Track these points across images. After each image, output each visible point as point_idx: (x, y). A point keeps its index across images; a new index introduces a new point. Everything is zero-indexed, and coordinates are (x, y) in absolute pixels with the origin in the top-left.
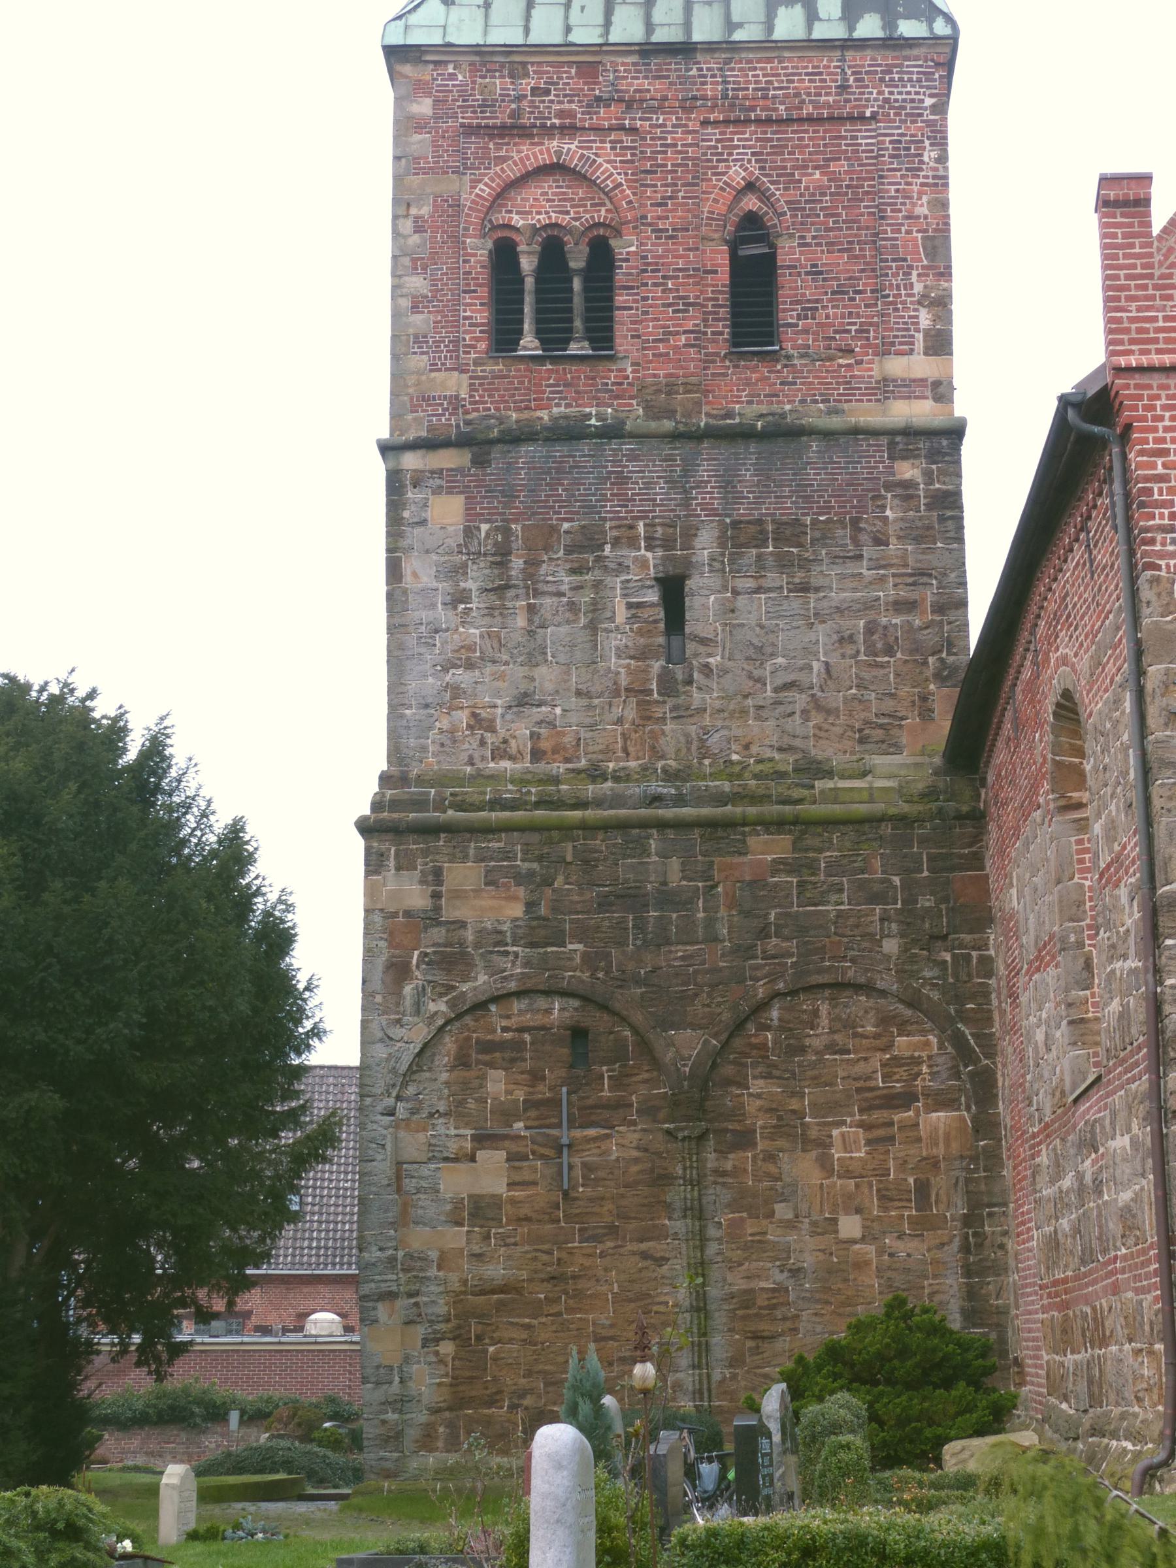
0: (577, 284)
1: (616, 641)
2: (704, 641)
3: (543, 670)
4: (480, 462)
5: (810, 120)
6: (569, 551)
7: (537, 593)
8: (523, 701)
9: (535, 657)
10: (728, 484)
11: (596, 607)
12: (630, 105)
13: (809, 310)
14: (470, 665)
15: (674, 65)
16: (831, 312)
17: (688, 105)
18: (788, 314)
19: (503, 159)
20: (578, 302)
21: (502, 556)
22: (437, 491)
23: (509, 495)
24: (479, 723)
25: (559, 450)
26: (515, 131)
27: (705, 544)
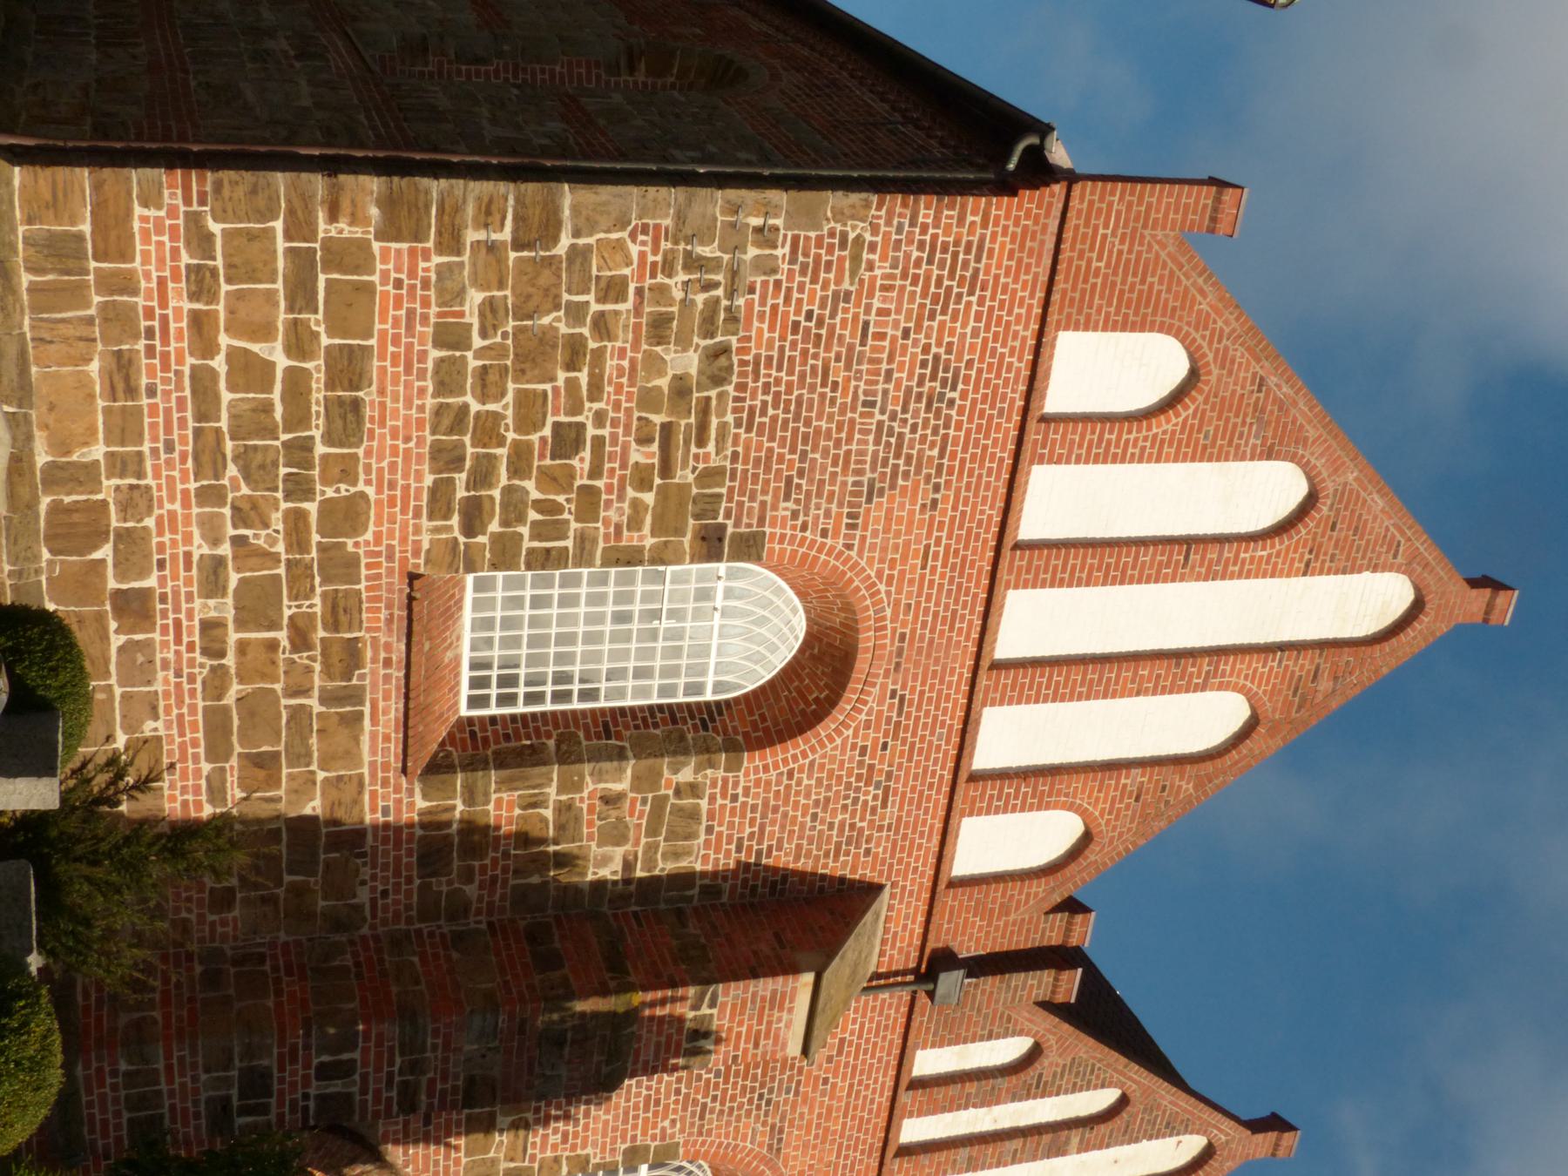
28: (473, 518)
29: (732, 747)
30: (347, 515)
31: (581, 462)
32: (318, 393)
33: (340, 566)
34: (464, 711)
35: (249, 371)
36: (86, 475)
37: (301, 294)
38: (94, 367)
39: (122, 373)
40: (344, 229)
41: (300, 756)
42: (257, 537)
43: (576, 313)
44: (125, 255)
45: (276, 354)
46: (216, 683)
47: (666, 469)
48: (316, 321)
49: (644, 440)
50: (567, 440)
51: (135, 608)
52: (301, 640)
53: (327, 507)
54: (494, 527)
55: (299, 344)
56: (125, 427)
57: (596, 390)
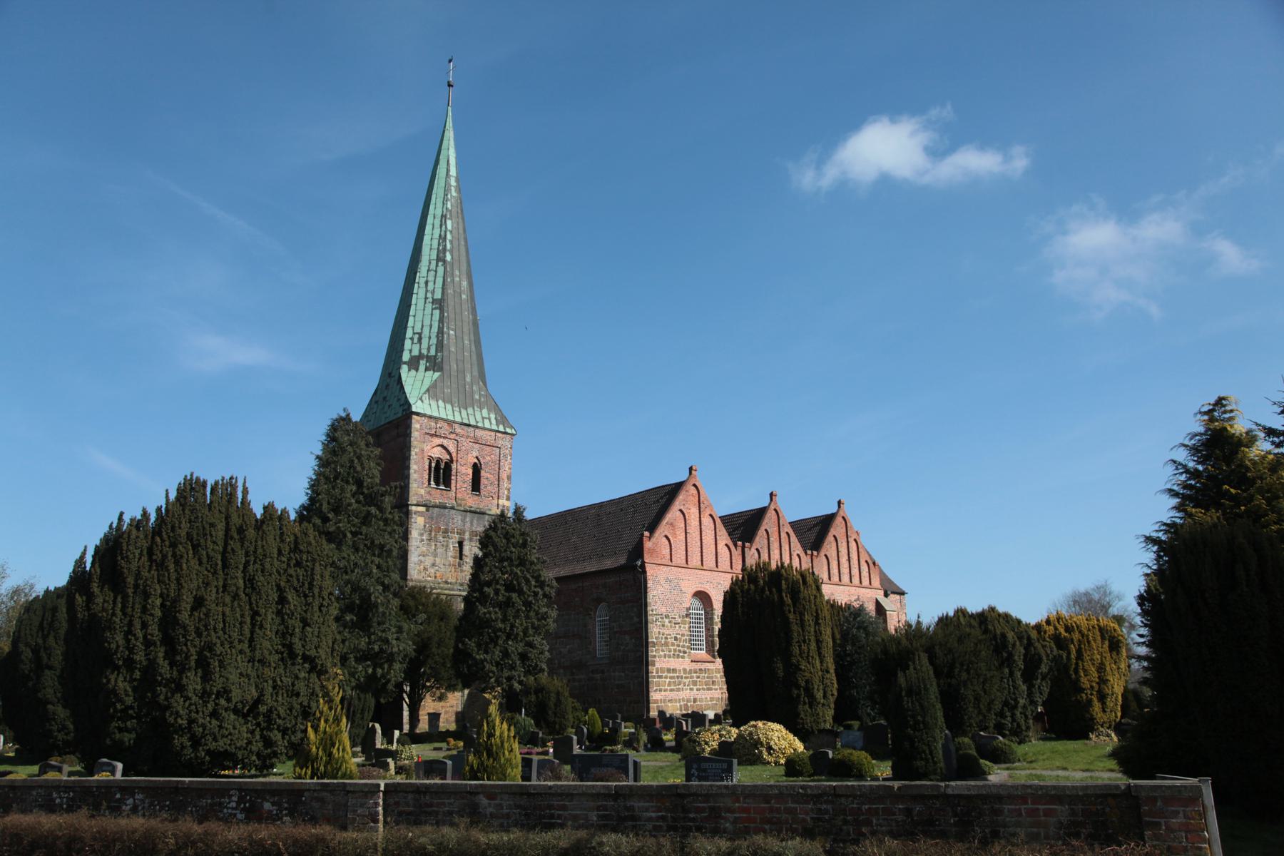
1: (450, 554)
4: (427, 510)
8: (434, 565)
9: (435, 555)
10: (472, 523)
11: (447, 546)
12: (457, 435)
13: (486, 487)
14: (424, 556)
15: (466, 428)
16: (490, 488)
17: (468, 437)
18: (482, 487)
21: (431, 531)
24: (425, 569)
25: (442, 510)
27: (467, 536)
28: (685, 652)
29: (712, 610)
30: (685, 670)
31: (678, 636)
32: (671, 675)
33: (690, 672)
35: (669, 684)
36: (681, 706)
37: (661, 677)
45: (668, 680)
46: (703, 689)
50: (676, 639)
51: (695, 700)
55: (666, 677)
56: (676, 701)
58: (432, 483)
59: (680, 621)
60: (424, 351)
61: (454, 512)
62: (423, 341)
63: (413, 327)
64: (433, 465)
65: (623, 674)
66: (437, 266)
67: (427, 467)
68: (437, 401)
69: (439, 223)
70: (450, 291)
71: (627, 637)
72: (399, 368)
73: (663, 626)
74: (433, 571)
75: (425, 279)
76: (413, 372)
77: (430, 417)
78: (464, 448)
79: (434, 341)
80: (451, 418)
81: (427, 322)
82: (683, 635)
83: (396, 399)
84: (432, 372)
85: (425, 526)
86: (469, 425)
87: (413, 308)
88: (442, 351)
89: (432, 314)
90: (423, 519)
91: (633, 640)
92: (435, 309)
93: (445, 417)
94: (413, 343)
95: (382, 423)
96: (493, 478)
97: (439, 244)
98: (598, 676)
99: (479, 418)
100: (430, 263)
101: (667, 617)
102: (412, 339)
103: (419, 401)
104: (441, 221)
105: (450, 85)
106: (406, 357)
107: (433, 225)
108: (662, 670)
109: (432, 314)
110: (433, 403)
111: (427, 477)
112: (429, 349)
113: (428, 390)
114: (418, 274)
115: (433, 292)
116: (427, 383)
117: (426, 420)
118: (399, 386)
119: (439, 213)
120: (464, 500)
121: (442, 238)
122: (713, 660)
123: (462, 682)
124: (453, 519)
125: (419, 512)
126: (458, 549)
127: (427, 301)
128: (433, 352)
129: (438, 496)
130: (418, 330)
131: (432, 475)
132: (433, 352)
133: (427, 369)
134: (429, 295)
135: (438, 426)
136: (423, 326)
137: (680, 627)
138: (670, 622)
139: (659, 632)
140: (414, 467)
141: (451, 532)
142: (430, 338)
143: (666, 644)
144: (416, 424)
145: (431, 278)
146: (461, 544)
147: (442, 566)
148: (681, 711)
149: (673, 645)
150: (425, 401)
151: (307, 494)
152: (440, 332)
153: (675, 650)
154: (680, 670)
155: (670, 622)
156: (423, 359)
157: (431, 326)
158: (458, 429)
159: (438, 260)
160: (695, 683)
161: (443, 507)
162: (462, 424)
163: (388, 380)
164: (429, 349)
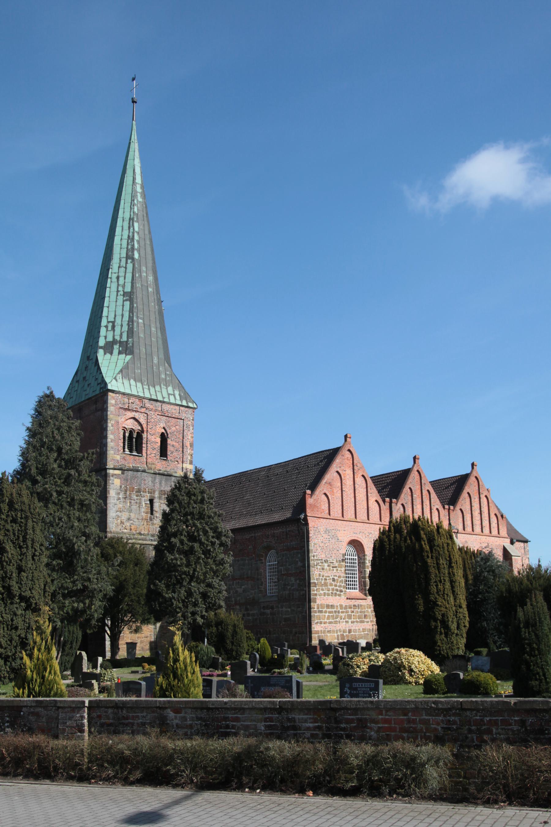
0: (134, 440)
1: (143, 510)
2: (156, 512)
3: (131, 514)
4: (123, 473)
5: (174, 418)
6: (136, 492)
7: (131, 500)
8: (129, 519)
9: (130, 511)
10: (160, 483)
11: (140, 503)
12: (147, 409)
13: (172, 453)
14: (120, 512)
16: (175, 454)
18: (169, 453)
19: (126, 415)
20: (134, 443)
21: (126, 491)
22: (116, 478)
23: (127, 480)
24: (122, 523)
25: (135, 473)
26: (128, 409)
27: (157, 495)
28: (341, 591)
29: (364, 555)
30: (341, 606)
31: (336, 578)
32: (330, 610)
34: (358, 591)
35: (328, 618)
36: (338, 636)
37: (321, 612)
38: (329, 635)
39: (329, 632)
40: (316, 607)
41: (364, 612)
42: (343, 617)
43: (322, 579)
44: (318, 631)
45: (327, 614)
46: (357, 622)
47: (336, 567)
48: (324, 610)
49: (333, 570)
50: (334, 580)
51: (350, 631)
52: (353, 612)
53: (341, 609)
54: (342, 588)
55: (326, 612)
56: (334, 631)
57: (329, 577)
58: (126, 450)
59: (337, 565)
60: (118, 338)
61: (145, 474)
62: (116, 328)
63: (107, 317)
64: (127, 435)
65: (289, 610)
66: (127, 263)
67: (122, 436)
68: (129, 380)
69: (128, 225)
70: (138, 285)
71: (293, 579)
72: (96, 352)
73: (323, 569)
74: (128, 524)
75: (116, 275)
76: (108, 356)
77: (124, 394)
78: (153, 420)
79: (125, 328)
80: (141, 394)
81: (119, 312)
82: (339, 577)
83: (94, 378)
84: (124, 355)
85: (121, 487)
86: (157, 401)
87: (107, 300)
88: (132, 337)
89: (123, 306)
90: (119, 480)
91: (298, 581)
92: (126, 300)
93: (137, 394)
94: (107, 330)
95: (83, 399)
96: (178, 446)
97: (128, 244)
98: (268, 611)
99: (165, 394)
100: (120, 260)
101: (326, 561)
102: (106, 327)
103: (114, 381)
104: (129, 223)
105: (134, 102)
106: (102, 342)
107: (122, 227)
108: (322, 606)
109: (123, 306)
110: (126, 382)
111: (122, 445)
112: (121, 337)
113: (121, 371)
114: (110, 270)
115: (124, 286)
116: (120, 365)
117: (120, 396)
118: (96, 367)
119: (127, 216)
120: (154, 464)
121: (131, 239)
122: (365, 597)
123: (154, 617)
124: (145, 480)
125: (115, 474)
126: (149, 506)
127: (119, 294)
128: (124, 338)
129: (131, 461)
130: (111, 319)
131: (126, 443)
132: (124, 338)
133: (120, 353)
134: (120, 289)
135: (130, 401)
136: (115, 316)
137: (337, 570)
138: (329, 566)
139: (320, 575)
140: (110, 437)
141: (143, 492)
142: (122, 326)
143: (325, 584)
144: (112, 399)
145: (122, 274)
146: (151, 501)
147: (136, 520)
148: (338, 639)
149: (331, 585)
150: (118, 380)
151: (20, 460)
152: (131, 320)
153: (333, 589)
154: (337, 606)
155: (329, 566)
156: (116, 344)
157: (123, 315)
158: (148, 404)
159: (127, 257)
160: (350, 617)
161: (136, 470)
162: (151, 400)
163: (87, 362)
164: (121, 337)
